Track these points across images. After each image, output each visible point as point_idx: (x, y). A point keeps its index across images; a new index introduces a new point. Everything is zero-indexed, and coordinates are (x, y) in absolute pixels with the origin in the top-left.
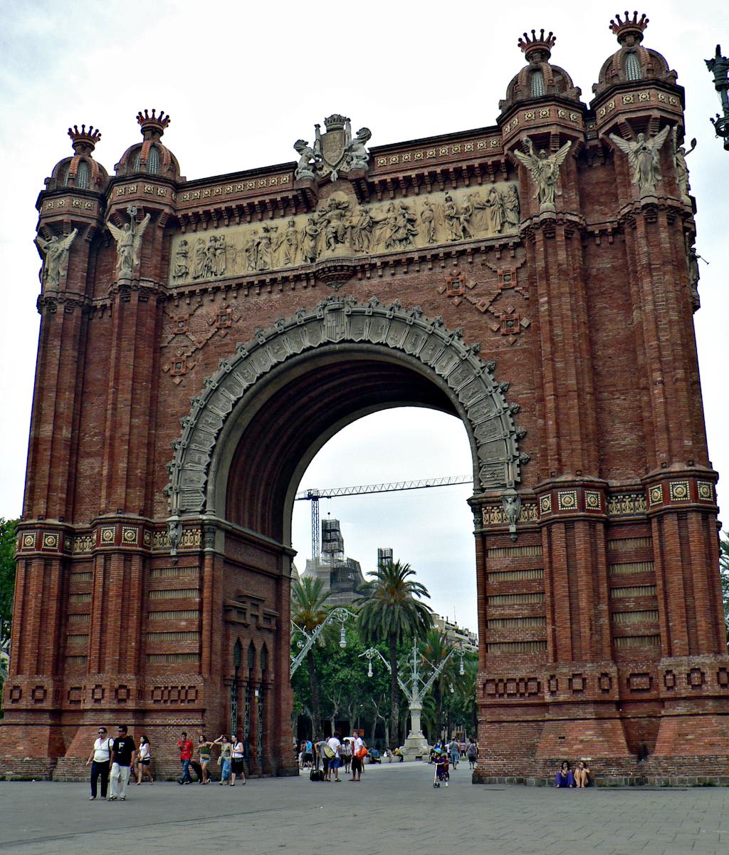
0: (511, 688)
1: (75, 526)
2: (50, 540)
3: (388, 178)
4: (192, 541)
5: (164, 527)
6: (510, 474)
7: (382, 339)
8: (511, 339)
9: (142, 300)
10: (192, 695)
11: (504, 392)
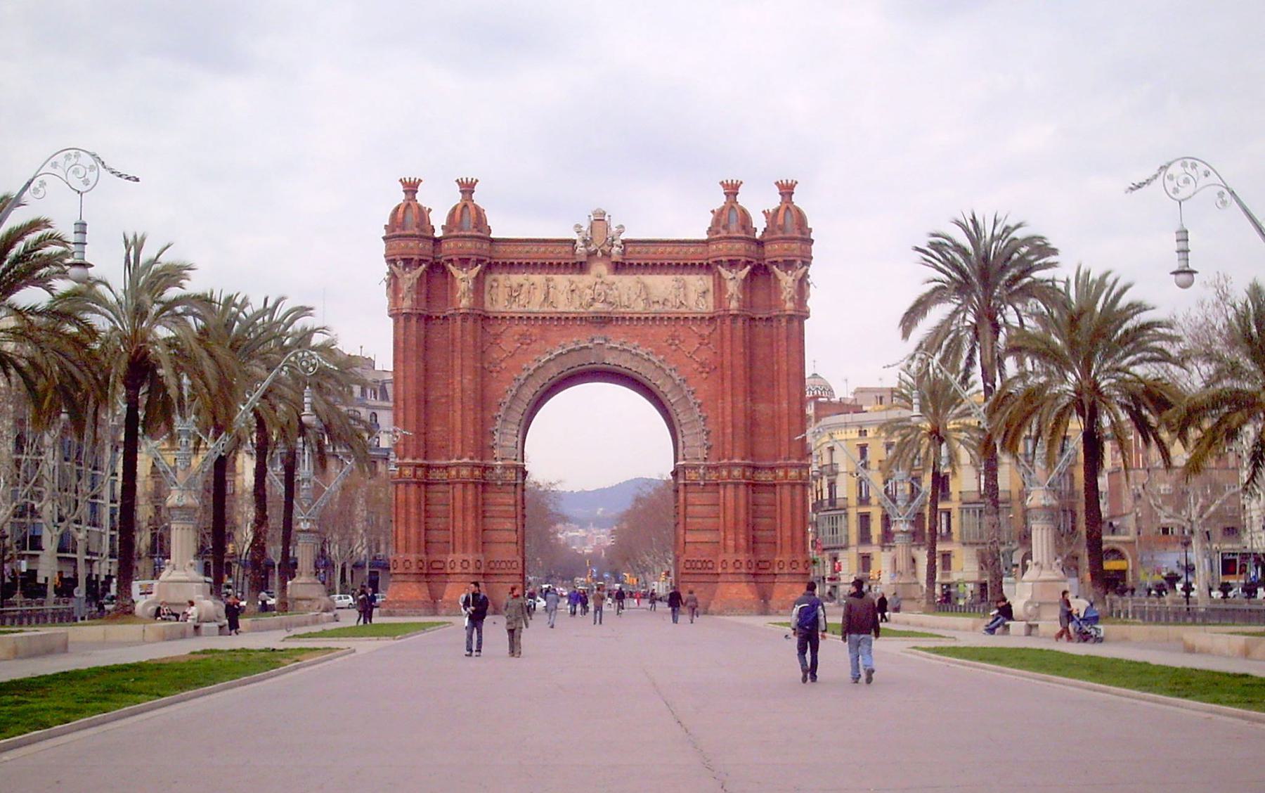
0: (699, 565)
1: (431, 462)
2: (419, 473)
3: (635, 263)
4: (511, 475)
5: (493, 468)
6: (702, 453)
7: (628, 365)
8: (704, 375)
9: (475, 321)
10: (514, 565)
11: (699, 406)
